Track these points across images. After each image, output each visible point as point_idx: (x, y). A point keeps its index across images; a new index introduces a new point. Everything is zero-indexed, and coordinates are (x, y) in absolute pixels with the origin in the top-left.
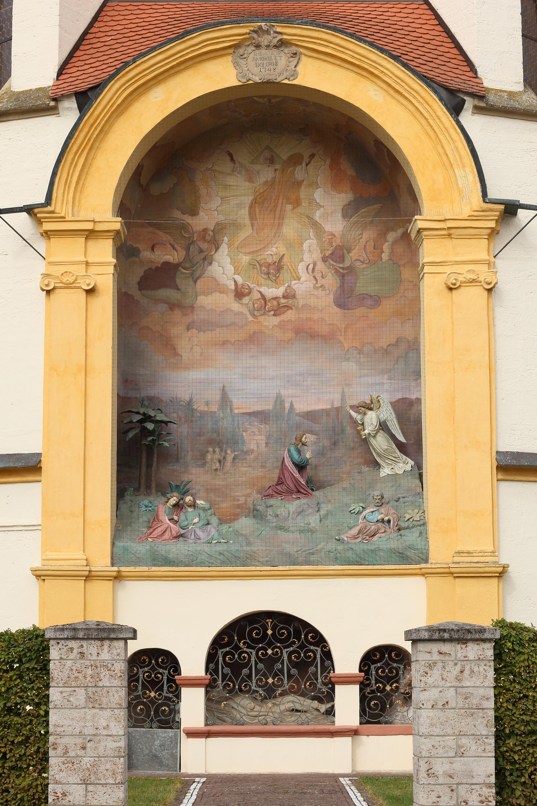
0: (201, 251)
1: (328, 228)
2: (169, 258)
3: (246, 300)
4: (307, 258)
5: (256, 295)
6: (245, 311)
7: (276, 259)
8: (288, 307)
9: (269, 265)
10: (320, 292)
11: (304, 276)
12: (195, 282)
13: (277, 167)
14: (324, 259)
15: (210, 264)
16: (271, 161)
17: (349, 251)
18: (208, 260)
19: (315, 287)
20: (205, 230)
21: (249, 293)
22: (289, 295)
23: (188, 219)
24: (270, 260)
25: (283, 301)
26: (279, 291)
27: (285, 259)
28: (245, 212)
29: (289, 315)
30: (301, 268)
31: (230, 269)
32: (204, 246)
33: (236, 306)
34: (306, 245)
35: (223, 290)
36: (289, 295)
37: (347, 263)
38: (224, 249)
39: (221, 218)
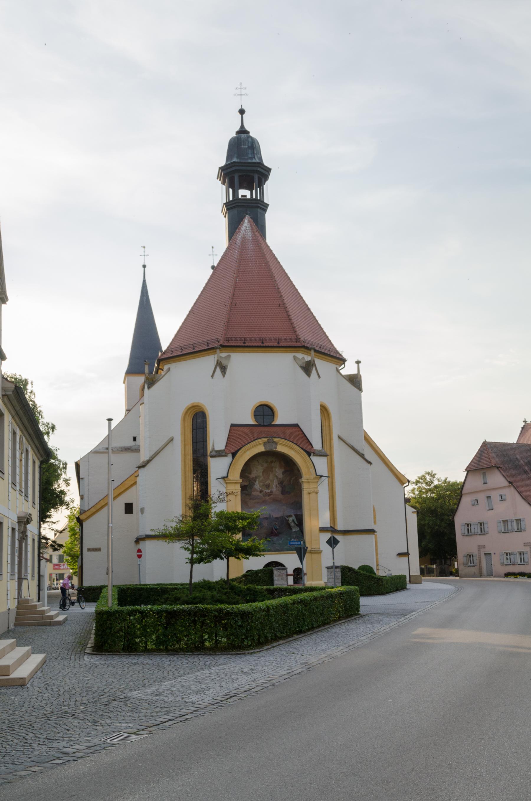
0: (252, 482)
1: (279, 477)
2: (245, 484)
3: (262, 493)
4: (275, 484)
5: (264, 492)
6: (262, 495)
7: (268, 484)
8: (271, 494)
9: (267, 485)
10: (278, 491)
11: (274, 488)
12: (251, 489)
13: (268, 463)
14: (279, 484)
15: (254, 485)
16: (267, 462)
17: (284, 482)
18: (254, 484)
19: (277, 490)
20: (253, 478)
21: (263, 491)
22: (271, 492)
23: (249, 475)
24: (267, 484)
25: (270, 493)
26: (269, 491)
27: (270, 484)
28: (261, 474)
29: (272, 496)
30: (274, 486)
31: (258, 486)
32: (253, 481)
33: (260, 495)
34: (274, 481)
35: (257, 491)
36: (271, 492)
37: (283, 485)
38: (257, 482)
39: (256, 475)
